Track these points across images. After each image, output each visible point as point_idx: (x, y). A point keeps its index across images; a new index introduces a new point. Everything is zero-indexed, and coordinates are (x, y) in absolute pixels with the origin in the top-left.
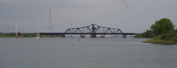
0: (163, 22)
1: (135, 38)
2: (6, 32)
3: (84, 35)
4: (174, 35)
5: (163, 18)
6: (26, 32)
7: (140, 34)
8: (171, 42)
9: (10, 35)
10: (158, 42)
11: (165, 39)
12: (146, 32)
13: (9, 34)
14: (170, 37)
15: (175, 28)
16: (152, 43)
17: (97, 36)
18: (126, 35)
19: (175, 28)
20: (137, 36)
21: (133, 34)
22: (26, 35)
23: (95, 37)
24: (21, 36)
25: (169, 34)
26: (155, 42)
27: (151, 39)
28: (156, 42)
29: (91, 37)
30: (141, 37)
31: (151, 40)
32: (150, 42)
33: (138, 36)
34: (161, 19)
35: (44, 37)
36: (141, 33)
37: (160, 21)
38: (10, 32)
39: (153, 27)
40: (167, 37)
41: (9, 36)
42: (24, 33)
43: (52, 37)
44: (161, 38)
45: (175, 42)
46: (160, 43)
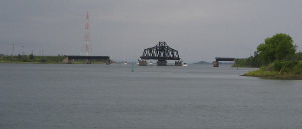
0: (278, 41)
1: (235, 66)
2: (9, 55)
3: (145, 60)
4: (296, 64)
5: (279, 33)
6: (44, 55)
7: (243, 59)
8: (290, 74)
9: (15, 59)
10: (268, 76)
11: (280, 69)
12: (253, 56)
13: (14, 57)
14: (289, 66)
15: (298, 51)
16: (257, 76)
17: (169, 62)
18: (219, 62)
19: (298, 51)
20: (238, 63)
21: (231, 60)
22: (44, 60)
23: (165, 64)
24: (34, 61)
25: (287, 62)
26: (262, 75)
27: (258, 69)
28: (264, 75)
29: (158, 64)
30: (244, 64)
31: (258, 71)
32: (254, 75)
33: (239, 63)
34: (275, 35)
35: (76, 63)
36: (245, 58)
37: (272, 38)
38: (16, 54)
39: (261, 49)
40: (284, 67)
41: (15, 61)
42: (41, 55)
43: (90, 64)
44: (274, 68)
45: (298, 75)
46: (273, 77)
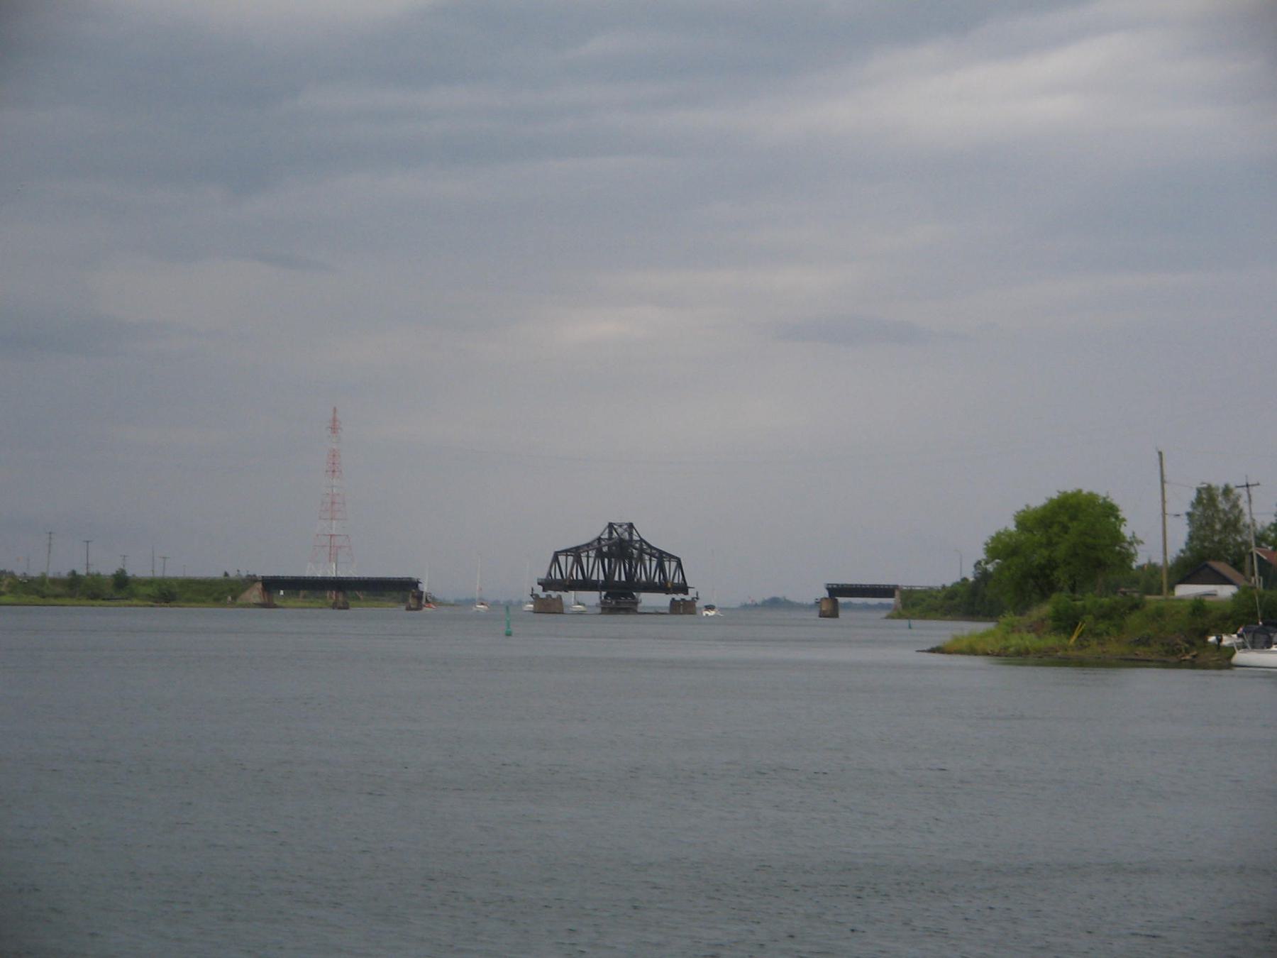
0: (1065, 519)
1: (900, 616)
2: (35, 572)
3: (554, 594)
4: (1135, 607)
5: (1070, 488)
6: (170, 573)
7: (931, 588)
9: (59, 590)
10: (1027, 652)
12: (971, 579)
13: (54, 581)
14: (1106, 615)
17: (648, 600)
18: (841, 600)
20: (914, 605)
23: (630, 608)
24: (132, 595)
26: (1006, 648)
28: (1012, 649)
29: (607, 609)
31: (989, 634)
32: (972, 651)
34: (1055, 496)
35: (290, 603)
37: (1044, 508)
38: (60, 567)
39: (1001, 548)
41: (57, 596)
42: (159, 574)
43: (346, 607)
45: (1141, 651)
46: (1046, 658)
